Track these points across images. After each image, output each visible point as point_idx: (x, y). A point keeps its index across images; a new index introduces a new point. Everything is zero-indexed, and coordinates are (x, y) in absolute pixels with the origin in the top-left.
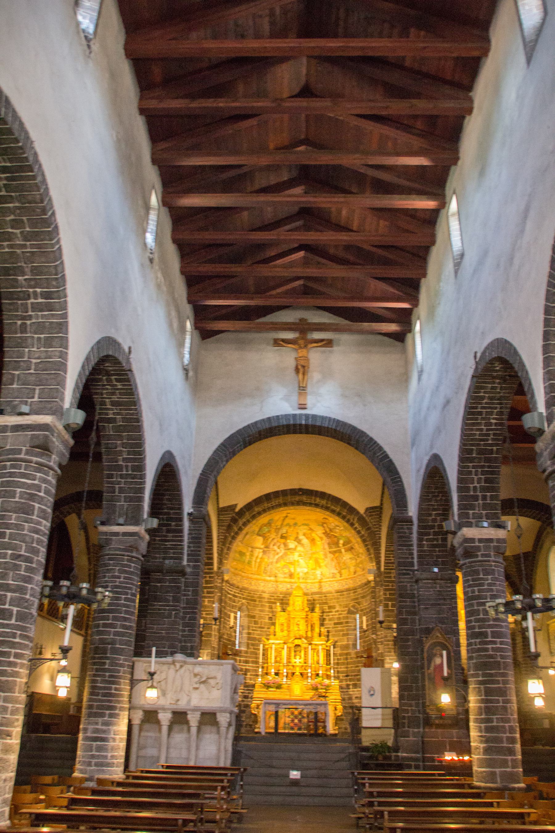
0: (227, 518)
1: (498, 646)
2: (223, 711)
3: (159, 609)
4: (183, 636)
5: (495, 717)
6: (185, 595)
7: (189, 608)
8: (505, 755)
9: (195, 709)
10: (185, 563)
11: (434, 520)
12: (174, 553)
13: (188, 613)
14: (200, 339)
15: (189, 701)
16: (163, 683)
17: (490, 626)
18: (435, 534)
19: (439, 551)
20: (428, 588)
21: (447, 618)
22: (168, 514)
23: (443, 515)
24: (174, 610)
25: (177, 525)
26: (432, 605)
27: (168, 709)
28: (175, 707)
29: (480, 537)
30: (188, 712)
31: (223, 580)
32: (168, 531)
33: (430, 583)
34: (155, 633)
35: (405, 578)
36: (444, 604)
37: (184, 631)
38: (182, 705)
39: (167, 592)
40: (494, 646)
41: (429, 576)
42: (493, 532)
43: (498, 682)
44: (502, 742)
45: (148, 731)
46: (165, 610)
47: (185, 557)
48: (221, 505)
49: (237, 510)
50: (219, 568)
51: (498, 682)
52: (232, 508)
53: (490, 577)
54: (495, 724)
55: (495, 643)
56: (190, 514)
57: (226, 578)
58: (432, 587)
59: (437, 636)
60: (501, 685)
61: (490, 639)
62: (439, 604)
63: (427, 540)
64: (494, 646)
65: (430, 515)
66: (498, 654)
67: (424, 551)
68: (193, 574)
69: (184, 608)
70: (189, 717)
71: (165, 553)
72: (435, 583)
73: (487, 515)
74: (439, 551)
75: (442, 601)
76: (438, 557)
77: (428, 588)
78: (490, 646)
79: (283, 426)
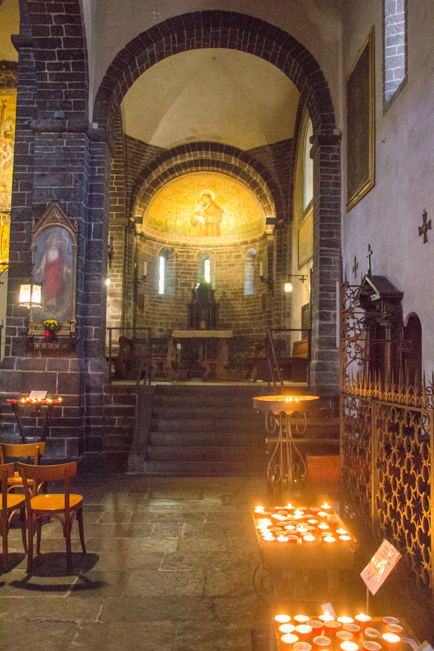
11: (57, 30)
18: (62, 55)
19: (70, 86)
20: (49, 144)
21: (74, 191)
23: (70, 19)
26: (54, 170)
33: (52, 136)
35: (25, 133)
36: (72, 169)
41: (49, 126)
58: (53, 144)
59: (54, 218)
62: (64, 170)
63: (51, 67)
65: (48, 20)
67: (47, 86)
72: (60, 137)
74: (70, 86)
75: (70, 165)
76: (69, 95)
77: (49, 144)
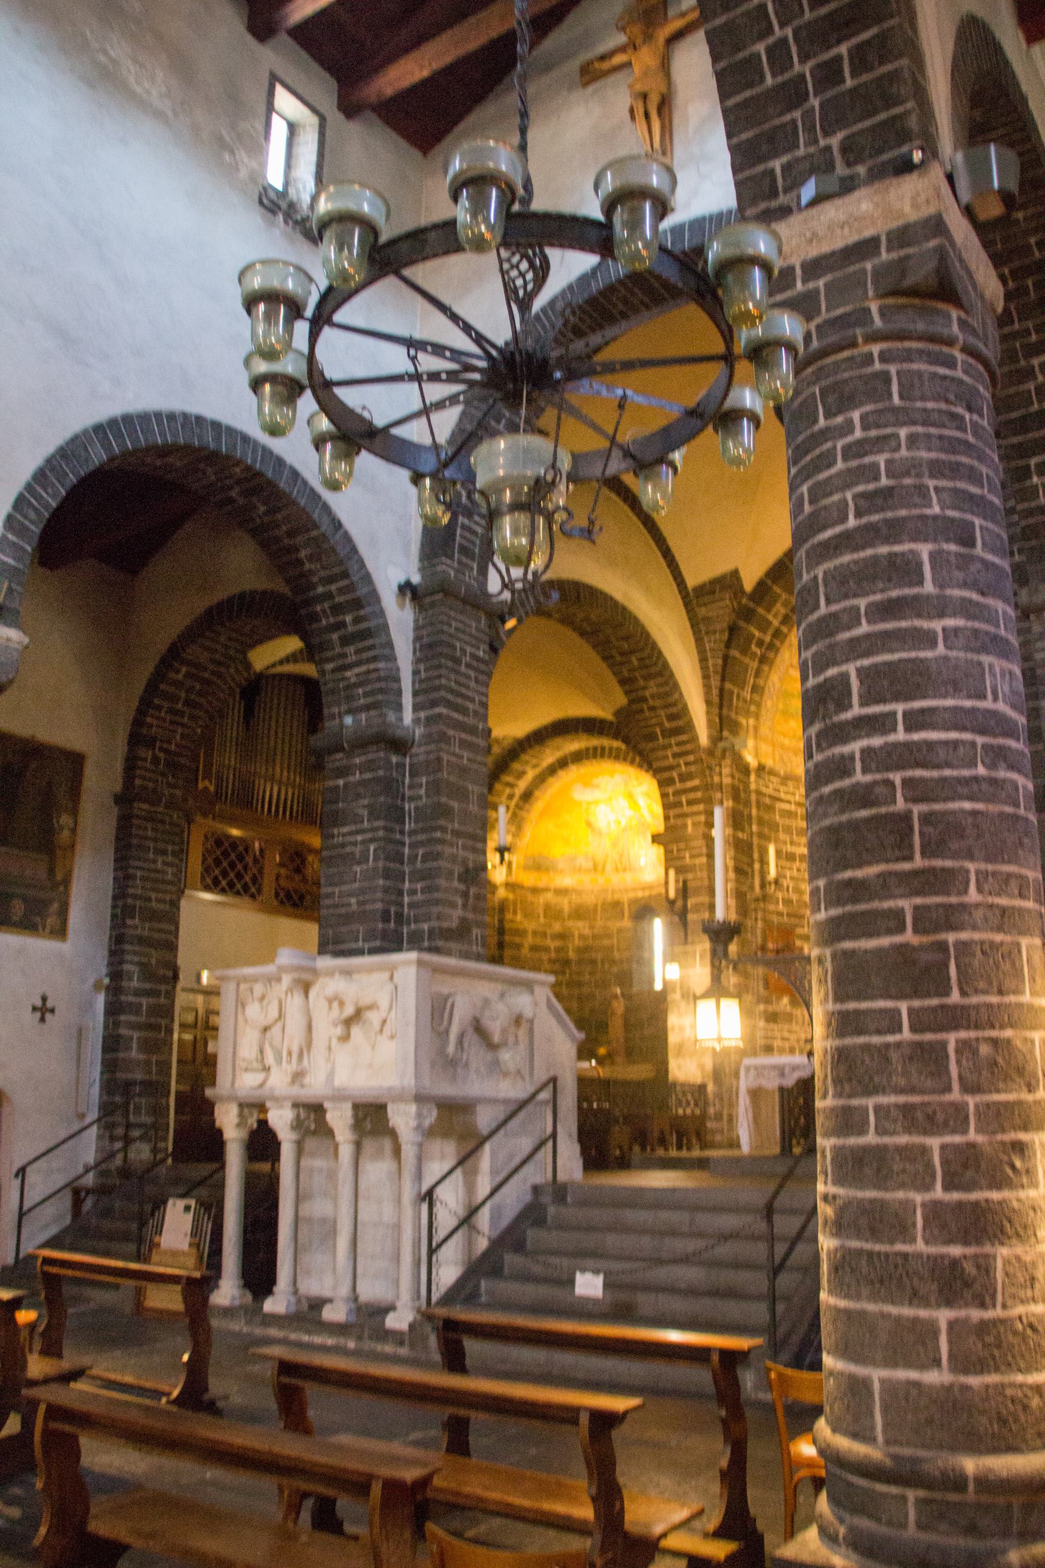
0: (721, 611)
1: (900, 735)
2: (400, 1097)
3: (343, 845)
4: (411, 905)
5: (870, 1102)
6: (411, 799)
7: (424, 830)
8: (925, 1302)
9: (339, 1097)
10: (408, 716)
12: (366, 694)
13: (422, 844)
14: (417, 154)
15: (331, 1074)
16: (276, 1030)
17: (857, 648)
22: (329, 596)
24: (372, 840)
25: (357, 620)
27: (285, 1098)
28: (296, 1091)
29: (814, 252)
30: (326, 1105)
31: (745, 770)
32: (345, 641)
34: (336, 906)
37: (413, 892)
38: (315, 1086)
39: (358, 796)
40: (877, 741)
42: (865, 206)
43: (895, 922)
44: (905, 1232)
45: (313, 1155)
46: (355, 844)
47: (407, 700)
48: (691, 582)
49: (749, 585)
50: (716, 739)
51: (895, 922)
52: (730, 581)
53: (856, 415)
54: (871, 1138)
55: (882, 724)
56: (406, 588)
57: (750, 759)
60: (909, 936)
61: (857, 710)
64: (877, 741)
66: (897, 777)
68: (428, 739)
69: (412, 833)
70: (329, 1117)
71: (350, 698)
73: (846, 148)
78: (855, 747)
79: (620, 282)
